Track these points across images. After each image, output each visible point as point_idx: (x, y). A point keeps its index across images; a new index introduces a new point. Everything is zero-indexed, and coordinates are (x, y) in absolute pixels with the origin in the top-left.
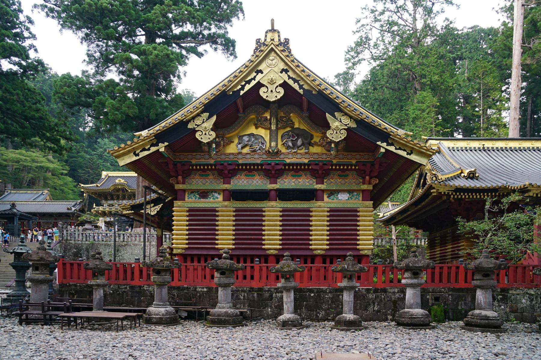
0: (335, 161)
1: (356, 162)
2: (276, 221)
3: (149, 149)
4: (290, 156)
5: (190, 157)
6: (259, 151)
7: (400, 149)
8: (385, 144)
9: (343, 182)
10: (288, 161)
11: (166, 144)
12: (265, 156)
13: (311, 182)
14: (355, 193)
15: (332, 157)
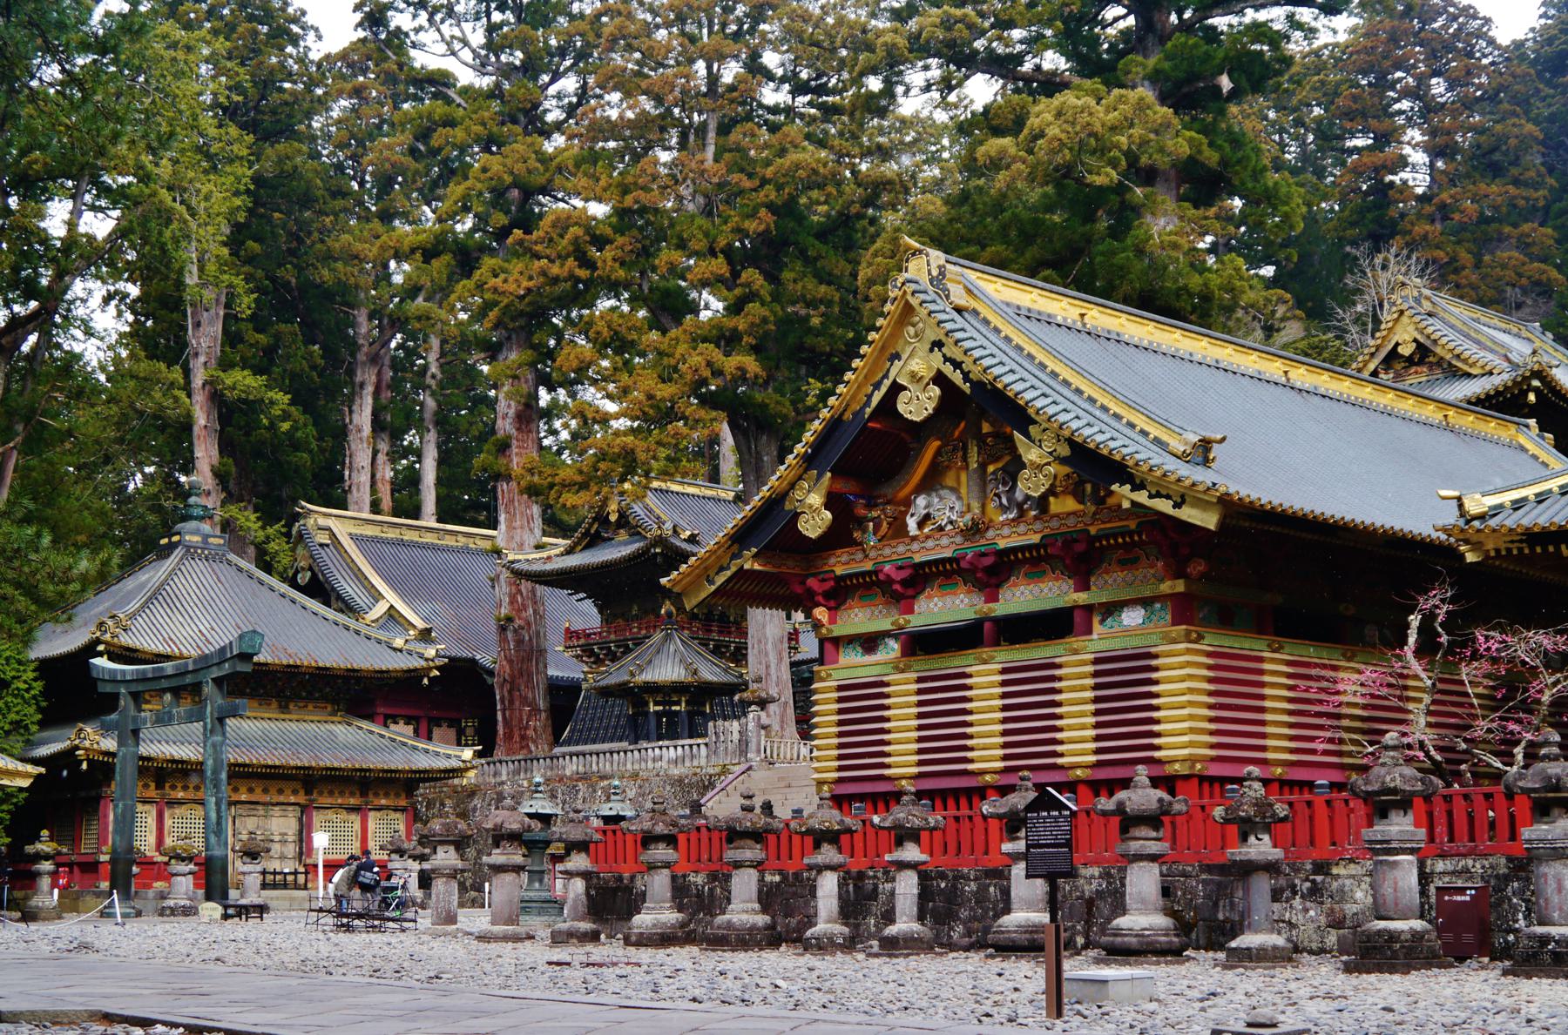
0: (1093, 530)
1: (1139, 525)
2: (991, 697)
3: (728, 568)
4: (1006, 531)
5: (832, 561)
6: (949, 527)
7: (1158, 495)
8: (1128, 487)
9: (1130, 578)
10: (1002, 544)
11: (754, 550)
12: (959, 539)
13: (1065, 587)
14: (1158, 606)
15: (1087, 520)
